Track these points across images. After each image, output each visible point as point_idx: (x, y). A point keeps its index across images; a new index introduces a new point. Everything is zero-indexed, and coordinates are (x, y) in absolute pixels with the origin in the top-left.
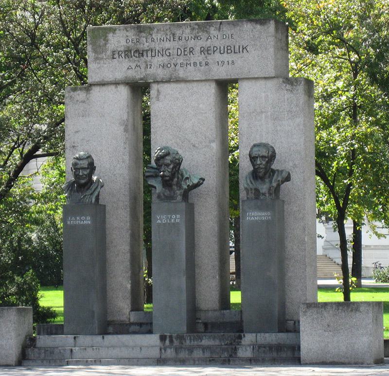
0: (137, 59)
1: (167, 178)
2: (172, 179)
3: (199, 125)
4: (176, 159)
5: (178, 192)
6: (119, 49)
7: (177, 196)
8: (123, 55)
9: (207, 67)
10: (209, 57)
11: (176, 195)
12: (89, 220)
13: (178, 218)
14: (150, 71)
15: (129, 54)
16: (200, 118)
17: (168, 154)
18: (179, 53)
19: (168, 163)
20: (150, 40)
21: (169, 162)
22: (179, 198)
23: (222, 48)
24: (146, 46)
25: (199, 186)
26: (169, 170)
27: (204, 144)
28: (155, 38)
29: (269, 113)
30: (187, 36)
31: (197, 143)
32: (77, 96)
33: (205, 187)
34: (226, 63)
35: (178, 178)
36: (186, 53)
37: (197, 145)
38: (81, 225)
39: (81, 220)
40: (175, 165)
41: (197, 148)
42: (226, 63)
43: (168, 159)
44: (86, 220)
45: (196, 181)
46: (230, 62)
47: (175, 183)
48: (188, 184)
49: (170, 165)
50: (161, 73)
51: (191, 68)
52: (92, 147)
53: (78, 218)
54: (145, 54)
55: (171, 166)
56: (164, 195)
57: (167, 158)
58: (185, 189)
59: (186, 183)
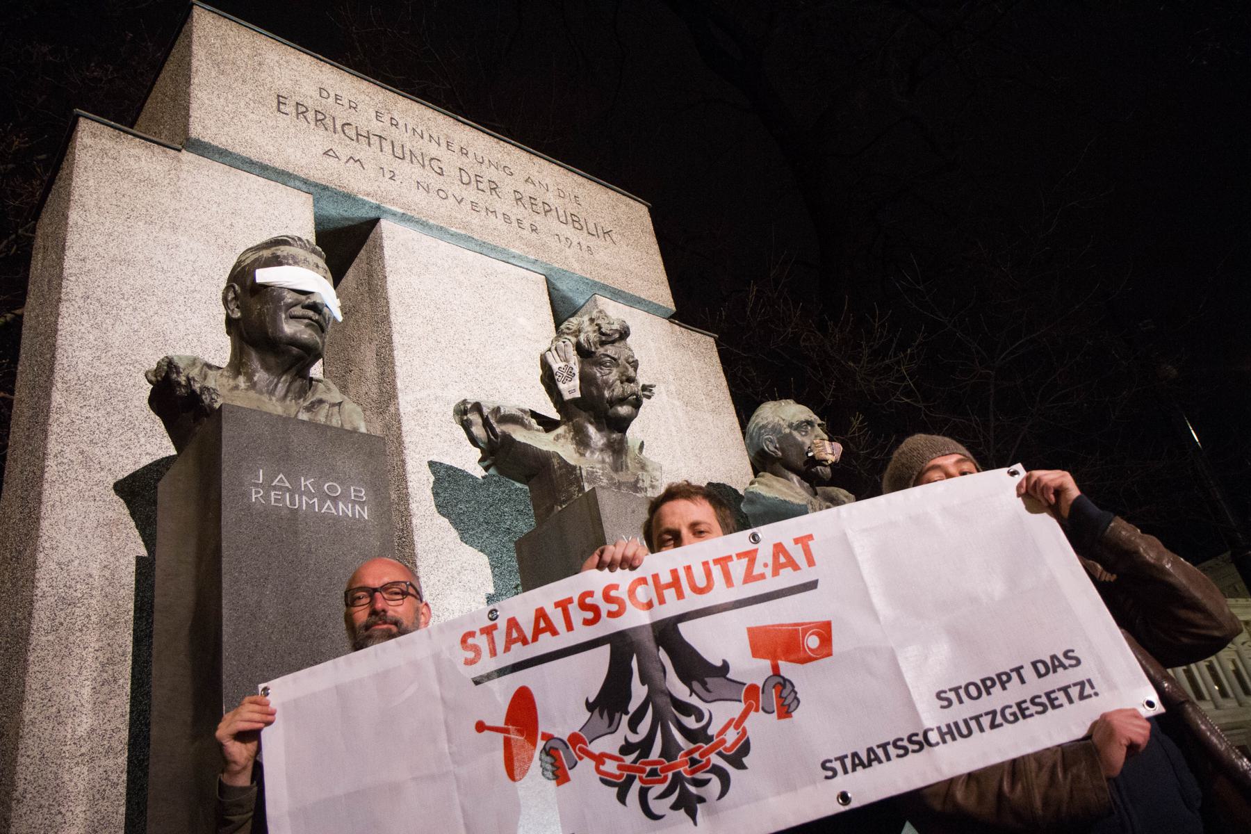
0: (354, 143)
6: (298, 99)
8: (311, 115)
9: (534, 234)
10: (537, 218)
12: (362, 504)
14: (392, 187)
15: (328, 121)
18: (466, 179)
20: (386, 118)
23: (561, 212)
24: (376, 127)
28: (401, 123)
29: (672, 388)
30: (479, 154)
32: (132, 161)
34: (575, 243)
36: (481, 186)
38: (324, 517)
39: (324, 497)
42: (575, 243)
44: (345, 497)
46: (584, 247)
50: (420, 202)
51: (499, 222)
52: (181, 327)
53: (306, 483)
54: (374, 140)
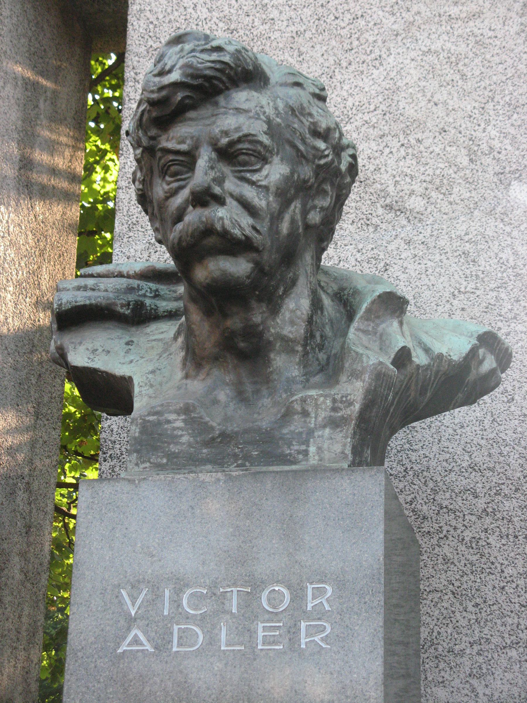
1: (239, 267)
2: (265, 288)
3: (432, 85)
4: (316, 133)
5: (319, 399)
7: (311, 433)
11: (296, 425)
13: (320, 614)
16: (437, 46)
17: (246, 74)
19: (246, 138)
21: (257, 128)
22: (333, 445)
25: (471, 399)
26: (259, 201)
27: (460, 191)
31: (418, 188)
33: (473, 467)
35: (316, 305)
37: (416, 203)
40: (306, 172)
41: (416, 217)
43: (242, 114)
45: (455, 346)
47: (288, 331)
48: (399, 342)
49: (263, 158)
55: (275, 172)
56: (196, 425)
57: (242, 97)
58: (380, 376)
59: (383, 342)
